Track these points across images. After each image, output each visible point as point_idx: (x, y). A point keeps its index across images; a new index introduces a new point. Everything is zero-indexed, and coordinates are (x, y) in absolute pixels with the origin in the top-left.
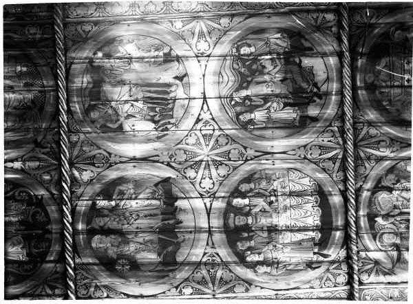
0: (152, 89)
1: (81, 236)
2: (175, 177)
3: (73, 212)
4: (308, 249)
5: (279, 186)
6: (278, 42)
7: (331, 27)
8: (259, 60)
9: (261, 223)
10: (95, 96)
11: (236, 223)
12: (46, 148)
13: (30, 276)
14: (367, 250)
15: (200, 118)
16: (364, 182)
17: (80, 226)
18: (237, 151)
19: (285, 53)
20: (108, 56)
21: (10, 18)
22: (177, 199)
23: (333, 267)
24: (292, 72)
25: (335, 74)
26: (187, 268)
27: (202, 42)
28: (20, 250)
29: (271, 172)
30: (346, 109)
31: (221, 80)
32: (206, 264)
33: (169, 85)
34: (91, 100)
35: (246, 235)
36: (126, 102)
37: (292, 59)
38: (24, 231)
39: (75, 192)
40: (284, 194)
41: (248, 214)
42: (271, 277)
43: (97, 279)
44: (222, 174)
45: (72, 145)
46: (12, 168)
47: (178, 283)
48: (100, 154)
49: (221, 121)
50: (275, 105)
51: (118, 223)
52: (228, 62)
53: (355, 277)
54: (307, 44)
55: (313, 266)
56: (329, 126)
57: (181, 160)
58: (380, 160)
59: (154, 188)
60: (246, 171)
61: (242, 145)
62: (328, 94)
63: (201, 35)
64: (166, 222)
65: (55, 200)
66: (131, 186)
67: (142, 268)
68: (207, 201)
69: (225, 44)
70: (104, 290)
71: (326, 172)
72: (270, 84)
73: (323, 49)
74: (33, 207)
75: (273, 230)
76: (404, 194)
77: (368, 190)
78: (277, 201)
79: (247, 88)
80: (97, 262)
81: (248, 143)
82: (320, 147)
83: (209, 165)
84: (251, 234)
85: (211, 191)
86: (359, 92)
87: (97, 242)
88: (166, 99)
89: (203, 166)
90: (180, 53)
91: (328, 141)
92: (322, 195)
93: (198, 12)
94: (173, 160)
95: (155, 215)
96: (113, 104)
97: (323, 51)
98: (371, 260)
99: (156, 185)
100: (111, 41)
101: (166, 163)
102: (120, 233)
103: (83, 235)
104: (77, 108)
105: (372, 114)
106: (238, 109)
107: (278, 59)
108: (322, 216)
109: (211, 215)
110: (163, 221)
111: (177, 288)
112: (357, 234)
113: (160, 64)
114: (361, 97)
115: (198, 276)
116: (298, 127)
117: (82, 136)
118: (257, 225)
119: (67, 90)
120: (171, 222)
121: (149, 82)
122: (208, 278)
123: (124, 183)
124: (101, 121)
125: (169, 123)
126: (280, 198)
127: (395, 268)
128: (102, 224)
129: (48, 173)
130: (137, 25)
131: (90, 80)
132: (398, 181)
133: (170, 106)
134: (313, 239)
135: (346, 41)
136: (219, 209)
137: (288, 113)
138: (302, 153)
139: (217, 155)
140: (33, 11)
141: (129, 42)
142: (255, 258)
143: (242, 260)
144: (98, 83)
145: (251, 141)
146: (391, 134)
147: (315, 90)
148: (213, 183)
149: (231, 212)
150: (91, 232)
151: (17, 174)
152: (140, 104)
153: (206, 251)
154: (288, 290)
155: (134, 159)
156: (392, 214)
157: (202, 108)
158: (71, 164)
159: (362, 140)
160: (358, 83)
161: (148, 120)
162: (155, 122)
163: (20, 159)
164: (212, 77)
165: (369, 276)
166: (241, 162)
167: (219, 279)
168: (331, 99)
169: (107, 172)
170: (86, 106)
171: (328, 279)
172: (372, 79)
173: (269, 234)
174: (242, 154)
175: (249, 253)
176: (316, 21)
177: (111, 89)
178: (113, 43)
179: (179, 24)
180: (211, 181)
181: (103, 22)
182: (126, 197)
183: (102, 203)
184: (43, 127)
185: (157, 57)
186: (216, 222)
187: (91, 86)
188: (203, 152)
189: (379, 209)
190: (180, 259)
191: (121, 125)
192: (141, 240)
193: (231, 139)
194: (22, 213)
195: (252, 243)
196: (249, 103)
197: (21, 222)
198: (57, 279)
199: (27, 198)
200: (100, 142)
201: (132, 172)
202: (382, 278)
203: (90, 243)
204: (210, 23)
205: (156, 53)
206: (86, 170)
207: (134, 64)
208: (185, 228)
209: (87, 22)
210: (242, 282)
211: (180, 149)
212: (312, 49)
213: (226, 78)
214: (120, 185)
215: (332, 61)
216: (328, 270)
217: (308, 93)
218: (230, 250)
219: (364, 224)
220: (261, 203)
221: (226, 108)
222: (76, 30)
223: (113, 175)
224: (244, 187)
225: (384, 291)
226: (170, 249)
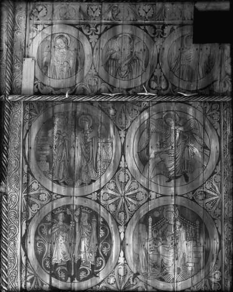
12: (133, 281)
13: (41, 265)
46: (120, 256)
65: (95, 286)
129: (115, 282)
194: (86, 262)
197: (80, 261)
198: (38, 284)
199: (97, 265)
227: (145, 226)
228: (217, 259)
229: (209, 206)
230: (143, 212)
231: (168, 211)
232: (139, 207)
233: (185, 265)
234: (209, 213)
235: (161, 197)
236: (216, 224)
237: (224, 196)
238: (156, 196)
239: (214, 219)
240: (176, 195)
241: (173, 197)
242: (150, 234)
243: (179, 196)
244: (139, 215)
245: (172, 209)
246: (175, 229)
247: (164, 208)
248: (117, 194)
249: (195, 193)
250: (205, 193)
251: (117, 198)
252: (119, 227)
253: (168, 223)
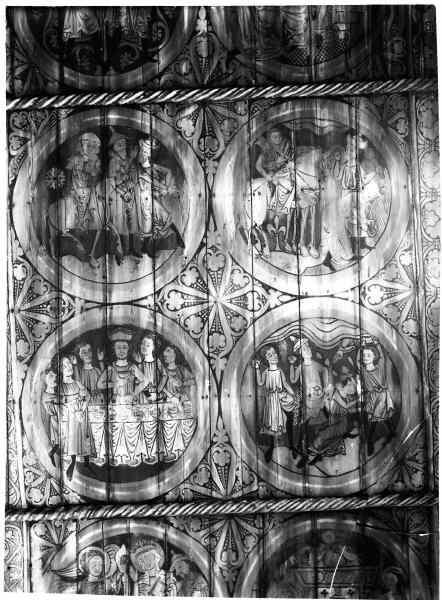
0: (313, 222)
1: (98, 118)
2: (185, 254)
3: (134, 106)
4: (80, 447)
5: (171, 406)
6: (381, 405)
7: (403, 481)
8: (355, 377)
9: (118, 379)
10: (302, 138)
11: (117, 343)
12: (227, 67)
13: (41, 44)
14: (79, 533)
15: (271, 291)
16: (178, 528)
17: (113, 117)
18: (222, 344)
19: (365, 414)
20: (361, 157)
21: (416, 15)
22: (153, 257)
23: (54, 484)
24: (337, 423)
25: (334, 486)
26: (52, 271)
27: (381, 294)
28: (79, 29)
29: (192, 393)
30: (284, 502)
31: (326, 321)
32: (58, 299)
33: (318, 245)
34: (296, 133)
35: (101, 357)
36: (294, 183)
37: (356, 424)
38: (107, 35)
39: (163, 108)
40: (160, 412)
41: (131, 360)
42: (39, 394)
43: (36, 141)
44: (188, 322)
45: (231, 105)
46: (198, 17)
47: (30, 259)
48: (218, 146)
49: (267, 321)
50: (290, 399)
51: (117, 172)
52: (352, 331)
53: (40, 516)
54: (378, 446)
55: (55, 455)
56: (259, 477)
57: (210, 263)
58: (210, 553)
59: (168, 224)
60: (194, 358)
61: (231, 352)
62: (305, 476)
63: (392, 293)
64: (119, 242)
65: (152, 80)
66: (172, 190)
67: (52, 206)
68: (150, 301)
69: (378, 327)
70: (20, 151)
71: (192, 474)
72: (320, 392)
73: (371, 469)
74: (141, 48)
75: (108, 396)
76: (160, 587)
77: (165, 535)
78: (150, 402)
79: (314, 358)
80: (62, 141)
81: (235, 360)
82: (228, 465)
83: (202, 303)
84: (102, 365)
85: (165, 307)
86: (309, 522)
87: (91, 142)
88: (297, 242)
89: (200, 295)
90: (365, 262)
91: (237, 477)
92: (158, 467)
93: (424, 288)
94: (210, 251)
95: (129, 226)
96: (291, 164)
97: (368, 470)
98: (64, 539)
99: (173, 227)
100: (382, 162)
101: (205, 241)
102: (103, 175)
103: (101, 121)
104: (286, 111)
105: (277, 540)
106: (284, 346)
107: (357, 404)
108: (127, 468)
109: (129, 307)
110: (121, 236)
111: (24, 257)
112: (102, 519)
113: (348, 233)
114: (301, 524)
115: (41, 288)
116: (257, 432)
117: (244, 119)
118: (115, 374)
119: (311, 98)
120: (119, 249)
121: (323, 217)
122: (38, 302)
123: (176, 181)
124: (265, 147)
125: (263, 246)
126: (154, 406)
127: (52, 574)
128: (116, 148)
130: (406, 199)
131: (326, 131)
132: (179, 578)
133: (288, 247)
134: (95, 455)
135: (381, 502)
136: (139, 319)
137: (277, 418)
138: (220, 438)
139: (217, 315)
140: (426, 49)
141: (381, 188)
142: (67, 371)
143: (64, 351)
144: (320, 142)
145: (237, 365)
146: (247, 569)
147: (311, 458)
148: (175, 310)
149: (134, 336)
150: (104, 133)
151: (189, 25)
152: (290, 203)
153: (77, 300)
154: (21, 418)
155: (211, 194)
156: (131, 569)
157: (284, 294)
158: (203, 104)
159: (239, 526)
160: (321, 521)
161: (268, 215)
162: (265, 225)
163: (210, 29)
164: (330, 308)
165: (41, 536)
166: (206, 350)
167: (37, 318)
168: (298, 480)
169: (191, 156)
170: (288, 125)
171: (36, 477)
172: (327, 541)
173: (102, 391)
174: (218, 351)
175: (75, 362)
176: (412, 459)
177: (313, 161)
178: (380, 163)
179: (406, 259)
180: (179, 307)
181: (411, 150)
182: (156, 183)
183: (147, 148)
184: (258, 63)
185: (359, 228)
186: (119, 314)
187: (317, 132)
188: (221, 295)
189: (138, 551)
190: (66, 261)
191: (261, 176)
192: (93, 205)
193: (240, 335)
194: (132, 32)
195: (88, 367)
196: (292, 362)
197: (118, 30)
198: (37, 83)
199: (154, 39)
200: (235, 145)
201: (192, 192)
202: (37, 555)
203: (89, 130)
204: (409, 305)
205: (365, 227)
206: (194, 125)
207: (349, 195)
208: (110, 268)
209: (410, 127)
210: (32, 351)
211: (225, 261)
212: (370, 453)
213: (328, 328)
214: (174, 174)
215: (354, 483)
216: (50, 477)
217: (307, 447)
218: (78, 334)
219: (117, 530)
220: (147, 379)
221: (285, 329)
222: (399, 111)
223: (188, 163)
224: (170, 355)
225: (19, 558)
226: (80, 247)
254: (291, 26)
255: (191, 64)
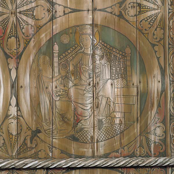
12: (31, 143)
46: (10, 105)
184: (54, 140)
227: (47, 58)
228: (159, 106)
229: (146, 25)
230: (44, 37)
231: (83, 34)
232: (39, 29)
233: (111, 117)
234: (146, 35)
235: (70, 12)
236: (156, 52)
237: (169, 9)
238: (64, 12)
239: (153, 45)
240: (94, 10)
241: (90, 12)
242: (56, 70)
243: (100, 10)
244: (39, 42)
245: (89, 31)
246: (94, 61)
247: (75, 31)
248: (5, 11)
249: (123, 6)
250: (139, 5)
251: (5, 16)
252: (9, 59)
253: (83, 52)
254: (79, 113)
255: (4, 139)
